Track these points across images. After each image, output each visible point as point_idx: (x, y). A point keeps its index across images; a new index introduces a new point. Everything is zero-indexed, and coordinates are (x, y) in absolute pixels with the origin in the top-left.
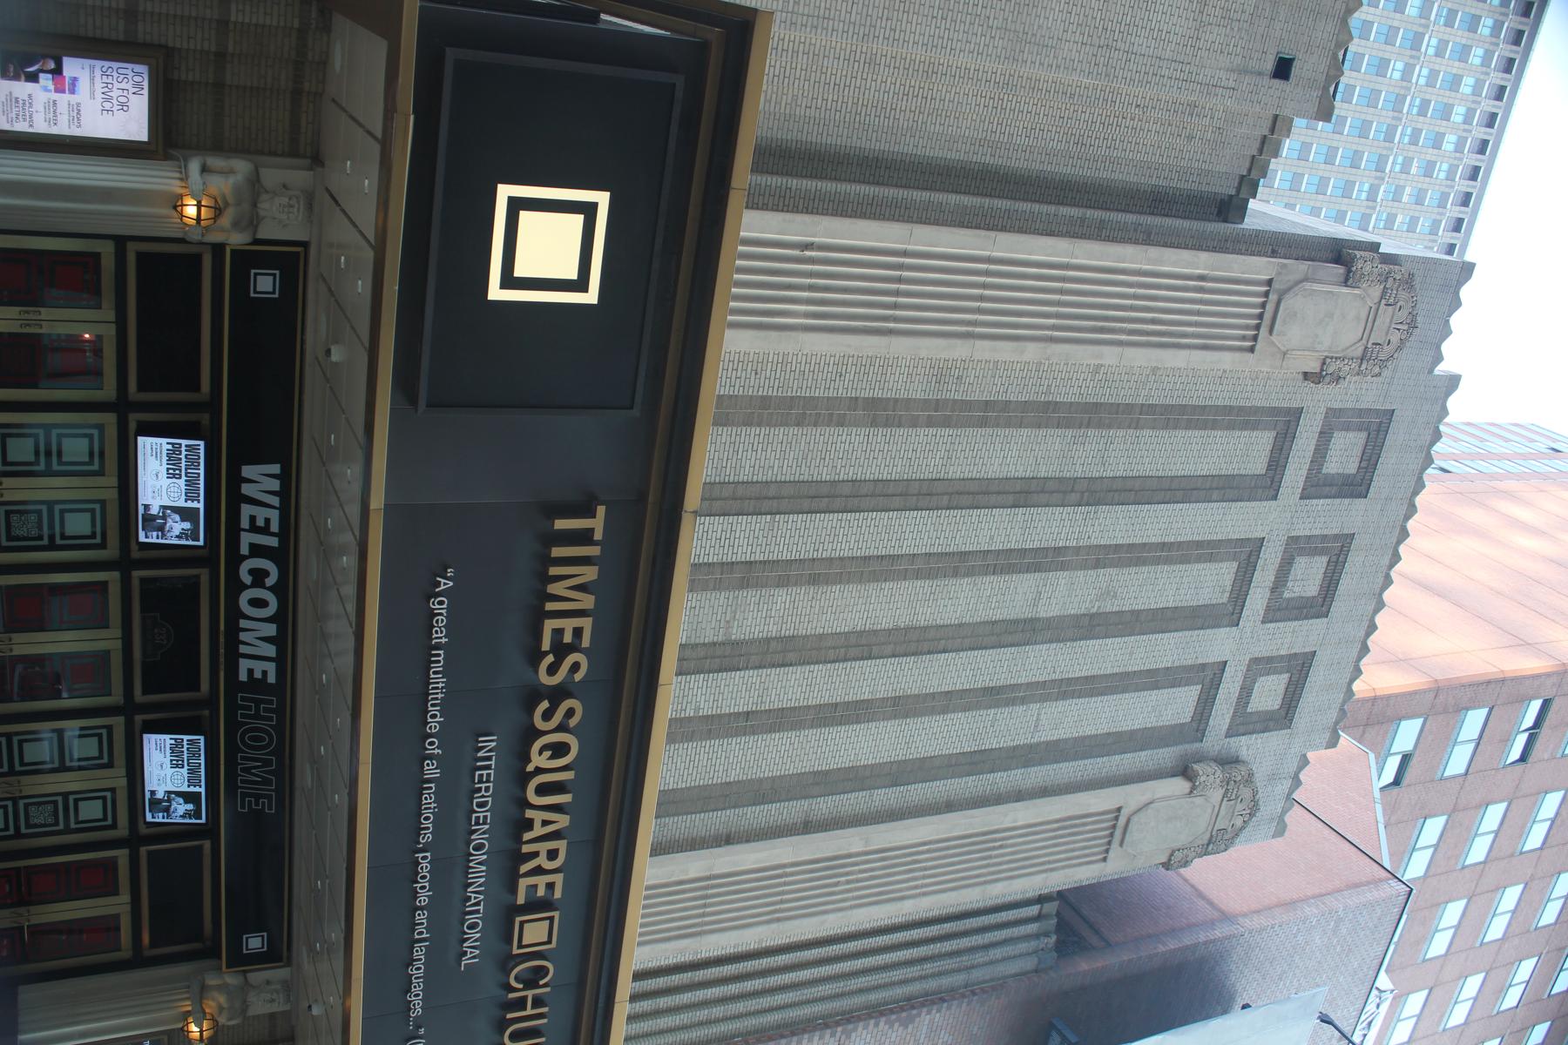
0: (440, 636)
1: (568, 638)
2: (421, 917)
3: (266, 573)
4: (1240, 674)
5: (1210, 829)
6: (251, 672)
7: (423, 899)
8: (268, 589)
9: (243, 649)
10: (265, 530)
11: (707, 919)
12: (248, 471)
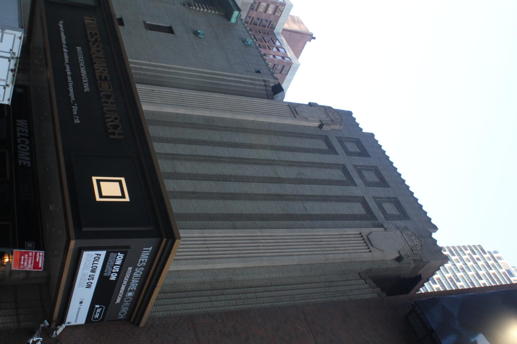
0: (62, 29)
1: (93, 34)
2: (69, 78)
3: (25, 141)
4: (372, 200)
5: (407, 244)
6: (22, 163)
7: (69, 73)
8: (28, 145)
9: (19, 158)
10: (24, 132)
11: (211, 253)
12: (18, 121)
